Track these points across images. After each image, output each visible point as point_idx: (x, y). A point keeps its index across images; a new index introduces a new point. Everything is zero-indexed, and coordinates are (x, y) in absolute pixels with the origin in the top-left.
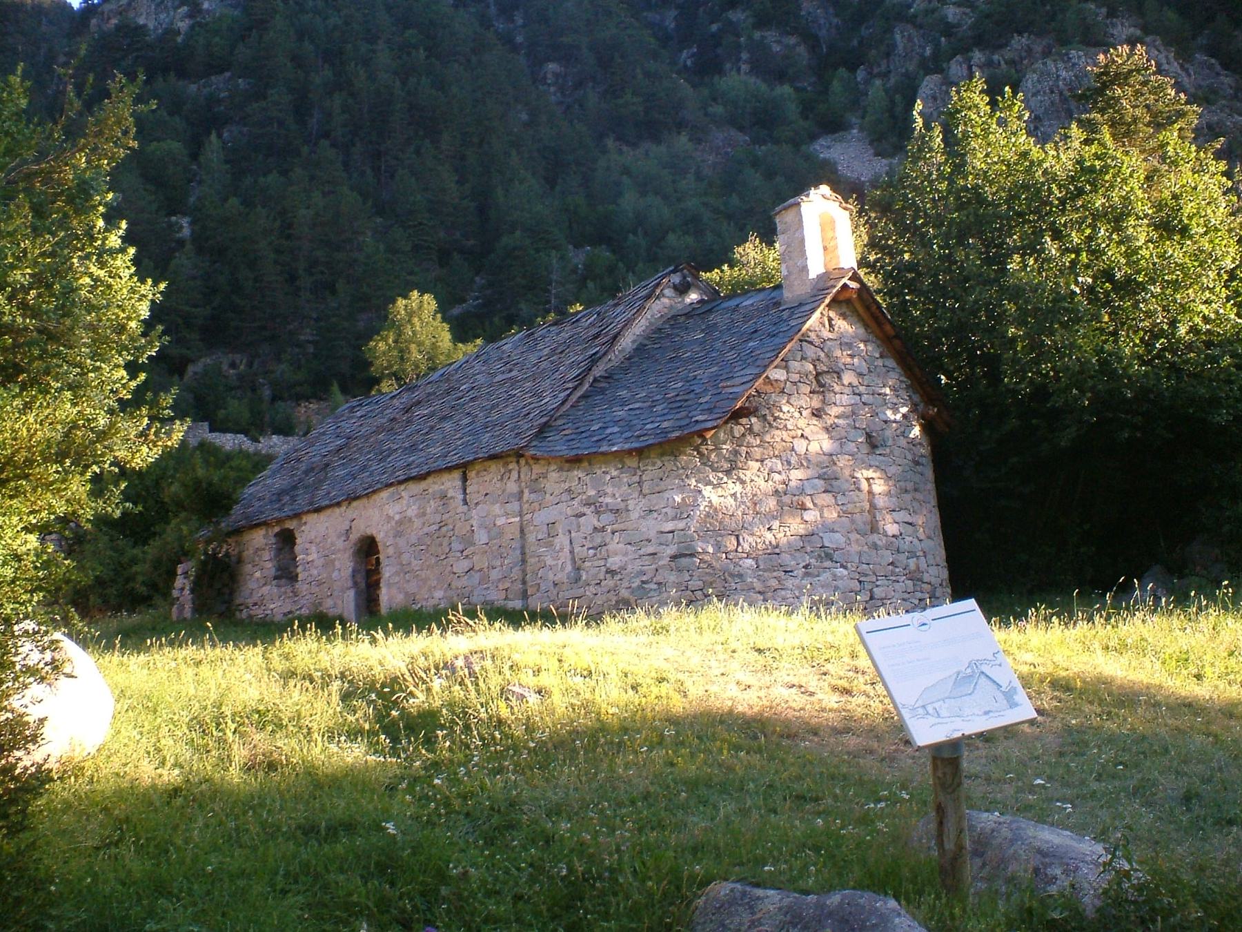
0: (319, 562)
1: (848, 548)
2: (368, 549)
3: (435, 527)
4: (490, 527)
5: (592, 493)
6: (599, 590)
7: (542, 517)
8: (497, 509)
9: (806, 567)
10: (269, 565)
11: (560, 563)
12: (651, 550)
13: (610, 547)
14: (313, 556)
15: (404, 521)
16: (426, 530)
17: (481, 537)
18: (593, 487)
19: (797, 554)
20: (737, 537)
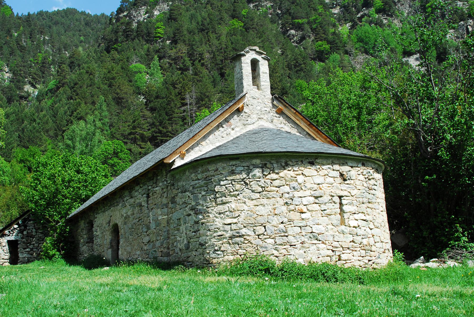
0: (100, 236)
1: (327, 233)
2: (116, 230)
3: (137, 220)
4: (156, 220)
5: (193, 204)
6: (197, 253)
7: (175, 216)
8: (159, 212)
9: (302, 243)
10: (85, 236)
11: (182, 239)
12: (220, 233)
13: (201, 232)
14: (98, 233)
15: (127, 217)
16: (134, 221)
17: (153, 226)
18: (194, 201)
19: (298, 236)
20: (265, 227)
